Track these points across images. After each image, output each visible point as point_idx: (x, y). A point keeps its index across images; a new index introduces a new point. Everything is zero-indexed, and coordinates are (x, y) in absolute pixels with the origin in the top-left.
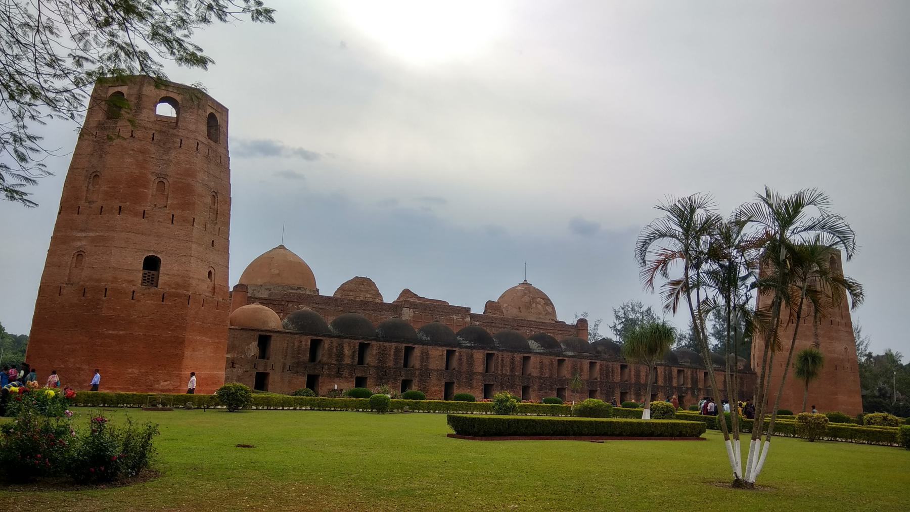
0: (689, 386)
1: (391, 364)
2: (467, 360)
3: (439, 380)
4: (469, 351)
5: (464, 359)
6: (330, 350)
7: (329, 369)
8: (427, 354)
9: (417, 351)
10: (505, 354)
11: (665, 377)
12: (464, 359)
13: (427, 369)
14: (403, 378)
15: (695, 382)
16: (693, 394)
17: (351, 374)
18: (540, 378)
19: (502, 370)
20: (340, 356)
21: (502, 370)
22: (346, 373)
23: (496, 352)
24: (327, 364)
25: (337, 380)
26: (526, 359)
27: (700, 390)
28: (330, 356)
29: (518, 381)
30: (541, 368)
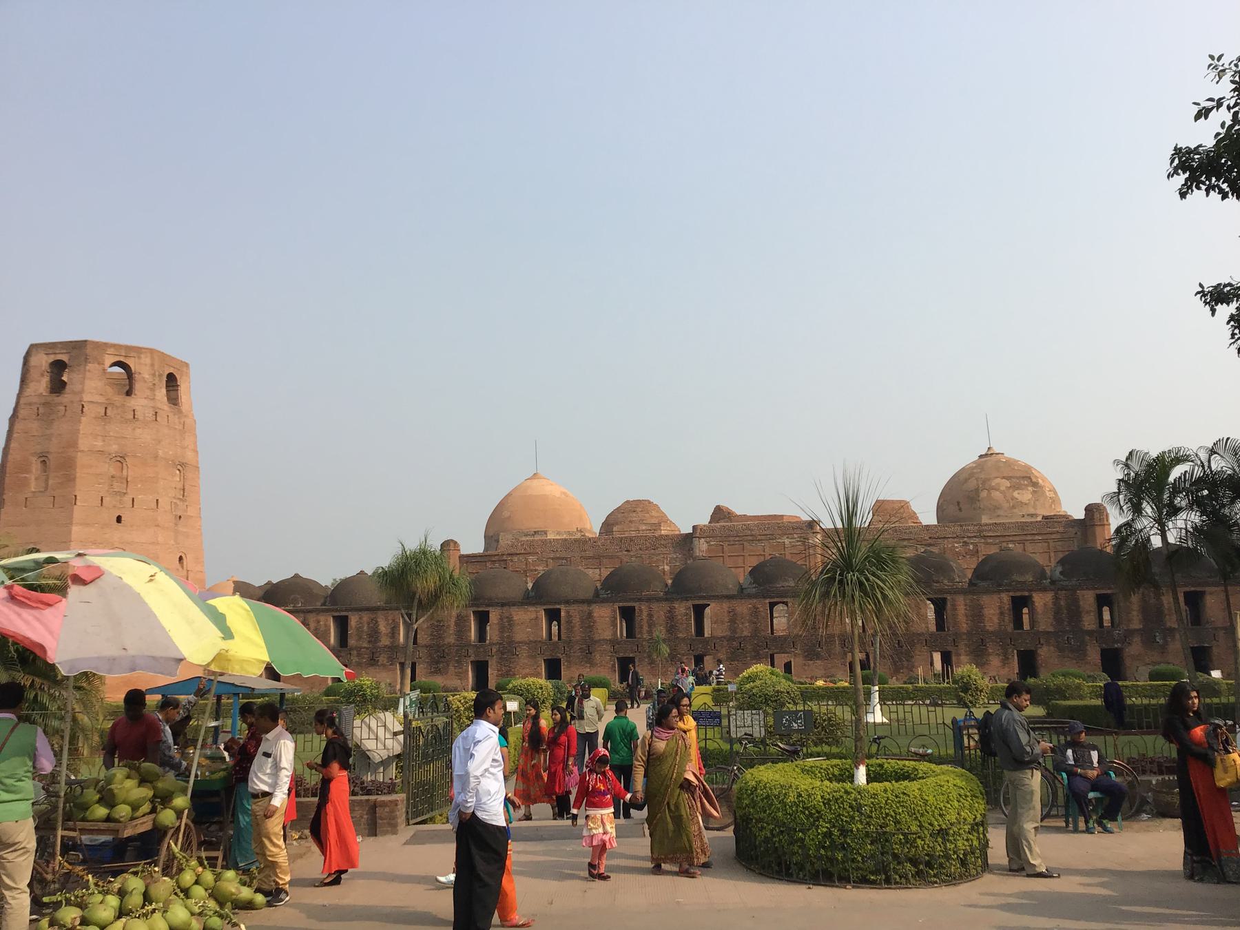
0: (1136, 624)
1: (450, 639)
2: (582, 621)
3: (533, 657)
4: (585, 607)
5: (576, 621)
6: (359, 629)
7: (359, 655)
8: (510, 619)
9: (494, 616)
10: (655, 606)
11: (1057, 613)
12: (576, 621)
13: (511, 642)
14: (472, 658)
15: (1153, 617)
16: (1149, 642)
17: (392, 660)
18: (730, 639)
19: (650, 632)
20: (374, 634)
21: (650, 632)
22: (383, 659)
23: (636, 605)
24: (356, 648)
25: (371, 669)
26: (699, 611)
27: (1172, 630)
28: (360, 638)
29: (683, 648)
30: (733, 621)
